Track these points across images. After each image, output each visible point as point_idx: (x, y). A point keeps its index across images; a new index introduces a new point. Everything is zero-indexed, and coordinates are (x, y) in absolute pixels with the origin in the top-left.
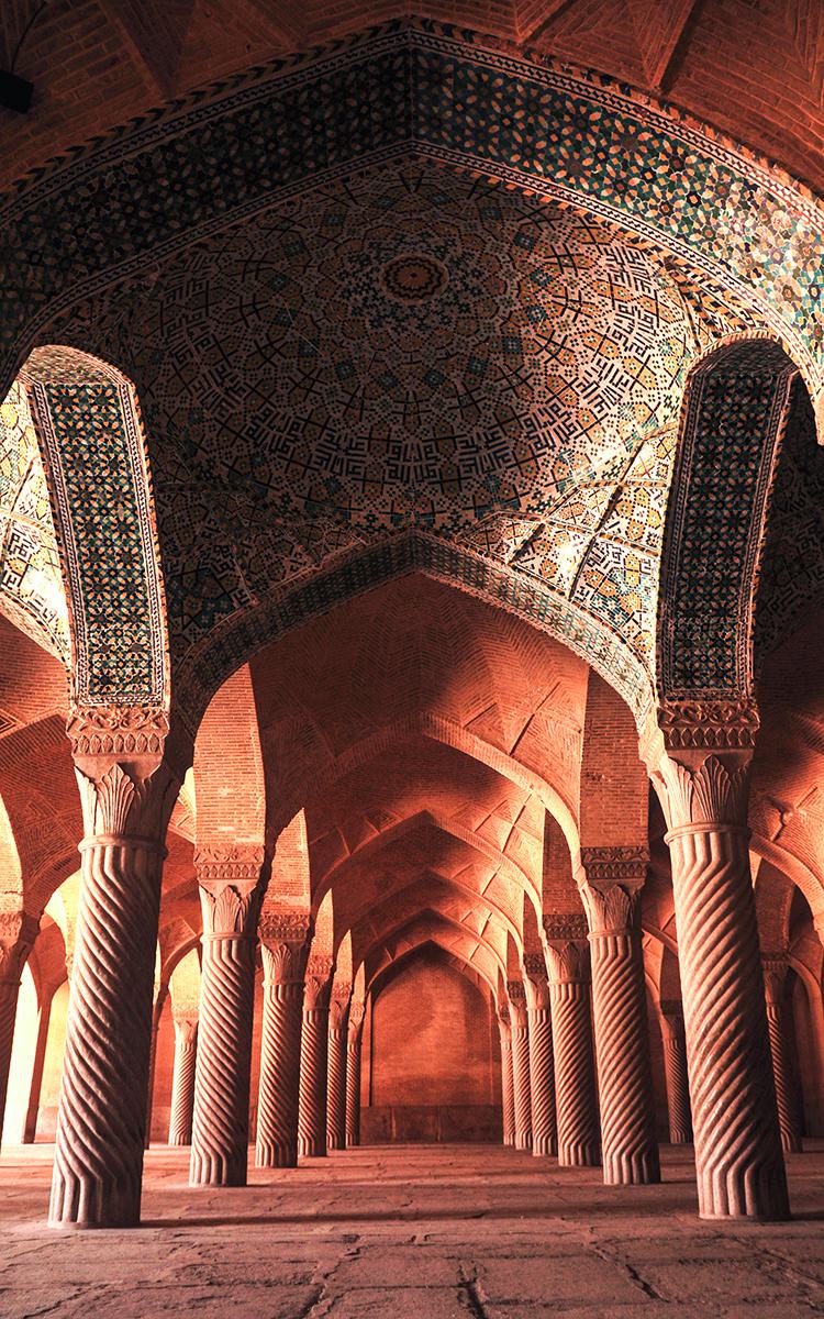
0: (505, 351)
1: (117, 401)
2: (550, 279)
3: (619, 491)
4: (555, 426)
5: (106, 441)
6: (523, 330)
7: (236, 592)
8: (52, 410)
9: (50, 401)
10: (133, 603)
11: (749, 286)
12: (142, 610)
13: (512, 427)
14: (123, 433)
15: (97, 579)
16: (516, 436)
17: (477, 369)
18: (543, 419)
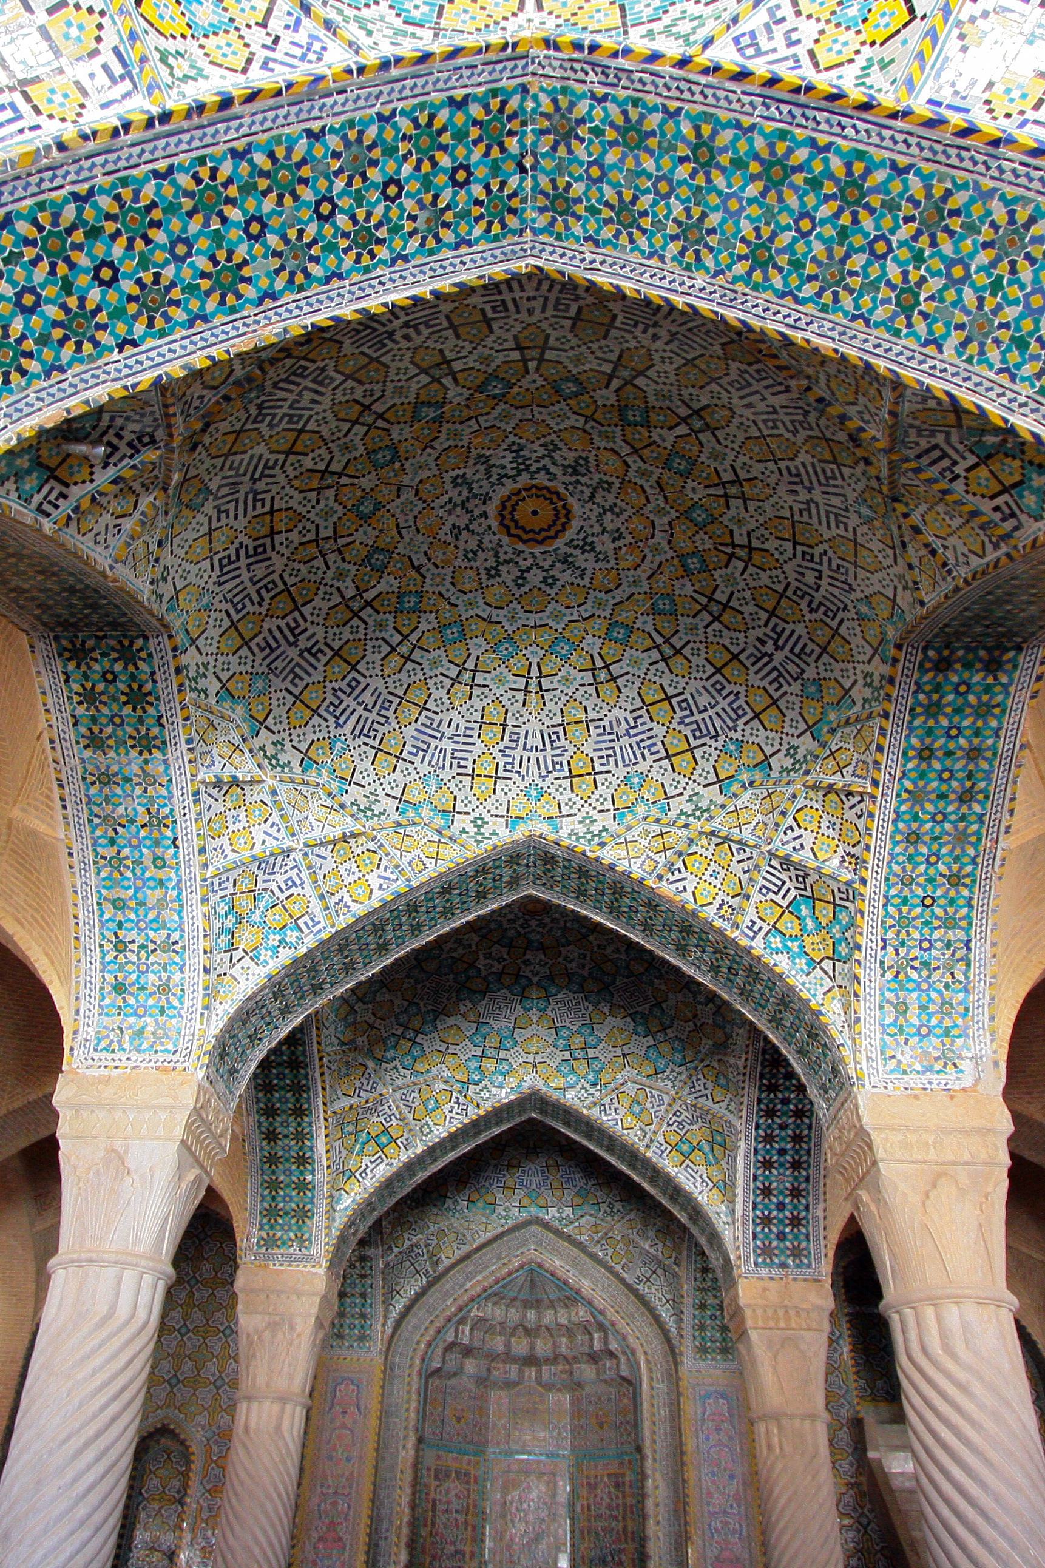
0: (441, 628)
1: (496, 238)
2: (565, 659)
3: (354, 835)
4: (366, 714)
5: (413, 218)
6: (481, 640)
7: (59, 488)
8: (476, 98)
9: (494, 93)
10: (43, 340)
11: (879, 972)
12: (33, 366)
13: (339, 667)
14: (431, 252)
15: (78, 236)
16: (330, 676)
17: (406, 605)
18: (367, 698)
